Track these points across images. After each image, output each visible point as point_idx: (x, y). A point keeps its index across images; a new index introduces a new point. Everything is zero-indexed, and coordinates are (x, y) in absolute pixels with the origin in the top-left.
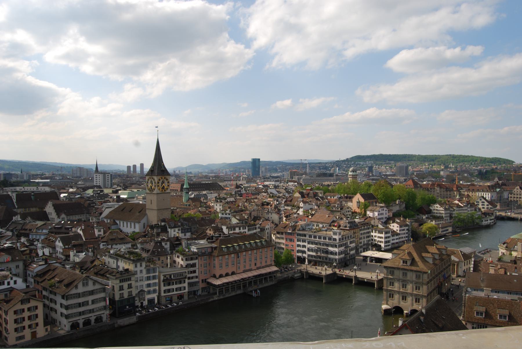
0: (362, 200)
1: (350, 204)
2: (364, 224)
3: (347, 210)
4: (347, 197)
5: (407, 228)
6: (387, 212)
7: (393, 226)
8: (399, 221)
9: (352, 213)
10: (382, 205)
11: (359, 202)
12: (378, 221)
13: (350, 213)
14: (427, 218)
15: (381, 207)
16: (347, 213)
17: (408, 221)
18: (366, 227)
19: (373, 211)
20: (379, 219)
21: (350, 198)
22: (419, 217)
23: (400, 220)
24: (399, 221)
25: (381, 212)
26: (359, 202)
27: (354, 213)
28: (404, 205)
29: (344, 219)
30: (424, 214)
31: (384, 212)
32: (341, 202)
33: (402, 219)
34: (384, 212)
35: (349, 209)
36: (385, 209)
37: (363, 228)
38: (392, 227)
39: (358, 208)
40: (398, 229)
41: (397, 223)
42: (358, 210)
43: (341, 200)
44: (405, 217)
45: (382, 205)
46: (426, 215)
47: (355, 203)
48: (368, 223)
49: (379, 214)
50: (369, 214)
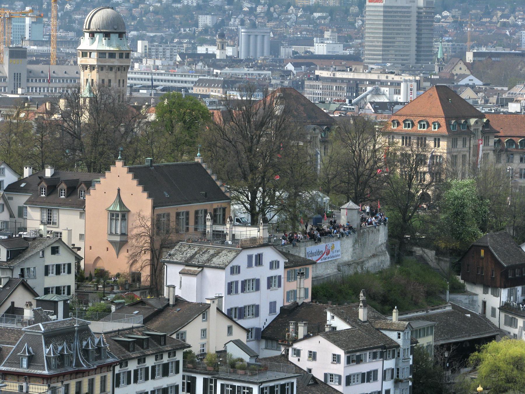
0: (141, 204)
1: (68, 222)
2: (131, 346)
3: (51, 260)
4: (52, 187)
5: (390, 364)
6: (281, 271)
7: (313, 356)
8: (341, 325)
9: (80, 278)
10: (253, 232)
11: (121, 214)
12: (227, 323)
13: (68, 280)
14: (505, 308)
15: (253, 243)
16: (53, 281)
17: (396, 328)
18: (150, 362)
19: (194, 266)
20: (235, 315)
21: (71, 193)
22: (461, 299)
23: (349, 317)
24: (341, 325)
25: (247, 273)
26: (121, 214)
27: (91, 280)
28: (381, 236)
29: (28, 314)
30: (491, 285)
31: (263, 273)
32: (22, 212)
33: (362, 314)
34: (263, 273)
35: (63, 258)
36: (269, 255)
37: (132, 366)
38: (304, 363)
39: (119, 246)
40: (341, 369)
41: (334, 336)
42: (117, 265)
43: (20, 200)
44: (383, 303)
45: (253, 232)
46: (504, 293)
47: (101, 222)
48: (160, 340)
49: (231, 288)
50: (179, 284)
